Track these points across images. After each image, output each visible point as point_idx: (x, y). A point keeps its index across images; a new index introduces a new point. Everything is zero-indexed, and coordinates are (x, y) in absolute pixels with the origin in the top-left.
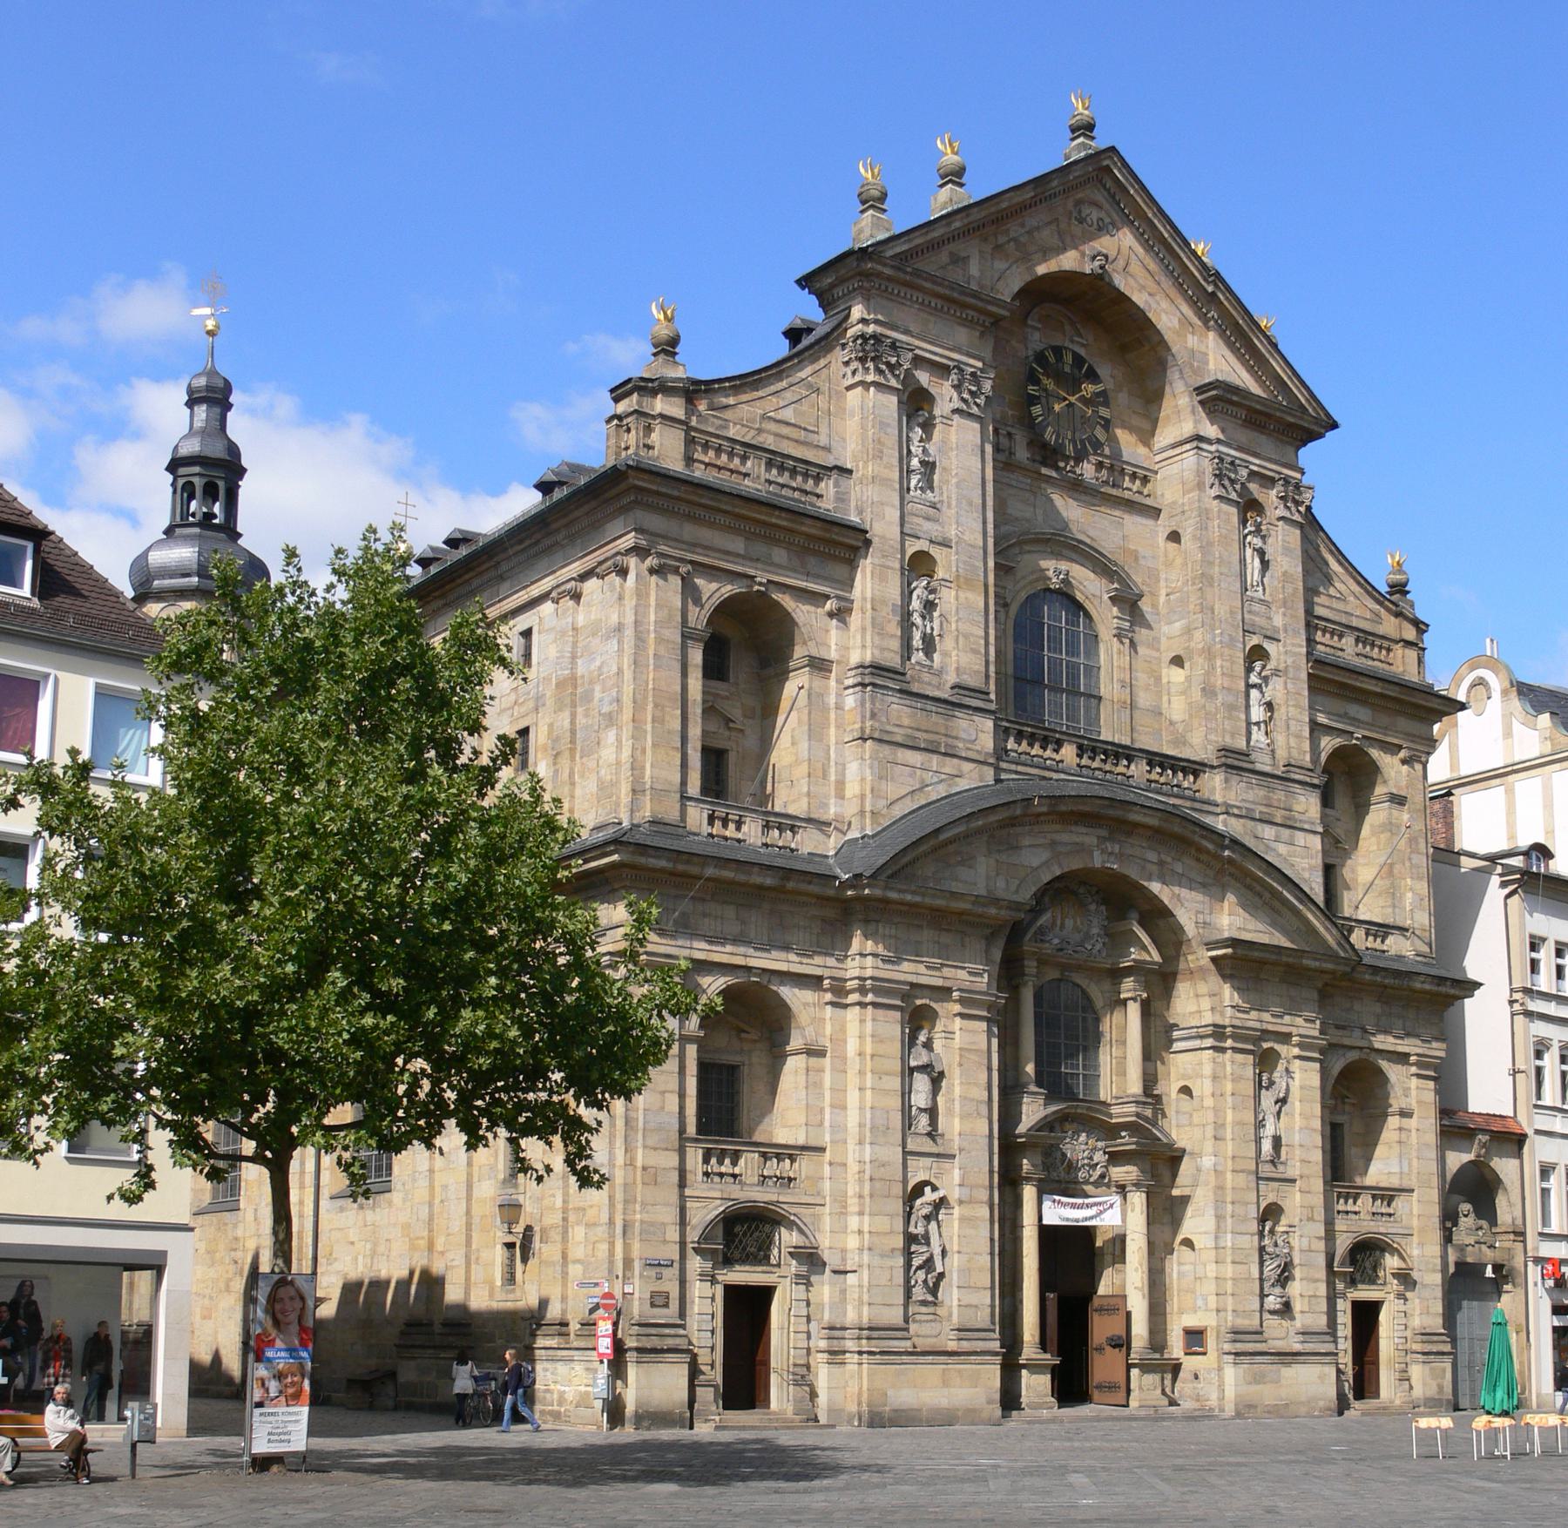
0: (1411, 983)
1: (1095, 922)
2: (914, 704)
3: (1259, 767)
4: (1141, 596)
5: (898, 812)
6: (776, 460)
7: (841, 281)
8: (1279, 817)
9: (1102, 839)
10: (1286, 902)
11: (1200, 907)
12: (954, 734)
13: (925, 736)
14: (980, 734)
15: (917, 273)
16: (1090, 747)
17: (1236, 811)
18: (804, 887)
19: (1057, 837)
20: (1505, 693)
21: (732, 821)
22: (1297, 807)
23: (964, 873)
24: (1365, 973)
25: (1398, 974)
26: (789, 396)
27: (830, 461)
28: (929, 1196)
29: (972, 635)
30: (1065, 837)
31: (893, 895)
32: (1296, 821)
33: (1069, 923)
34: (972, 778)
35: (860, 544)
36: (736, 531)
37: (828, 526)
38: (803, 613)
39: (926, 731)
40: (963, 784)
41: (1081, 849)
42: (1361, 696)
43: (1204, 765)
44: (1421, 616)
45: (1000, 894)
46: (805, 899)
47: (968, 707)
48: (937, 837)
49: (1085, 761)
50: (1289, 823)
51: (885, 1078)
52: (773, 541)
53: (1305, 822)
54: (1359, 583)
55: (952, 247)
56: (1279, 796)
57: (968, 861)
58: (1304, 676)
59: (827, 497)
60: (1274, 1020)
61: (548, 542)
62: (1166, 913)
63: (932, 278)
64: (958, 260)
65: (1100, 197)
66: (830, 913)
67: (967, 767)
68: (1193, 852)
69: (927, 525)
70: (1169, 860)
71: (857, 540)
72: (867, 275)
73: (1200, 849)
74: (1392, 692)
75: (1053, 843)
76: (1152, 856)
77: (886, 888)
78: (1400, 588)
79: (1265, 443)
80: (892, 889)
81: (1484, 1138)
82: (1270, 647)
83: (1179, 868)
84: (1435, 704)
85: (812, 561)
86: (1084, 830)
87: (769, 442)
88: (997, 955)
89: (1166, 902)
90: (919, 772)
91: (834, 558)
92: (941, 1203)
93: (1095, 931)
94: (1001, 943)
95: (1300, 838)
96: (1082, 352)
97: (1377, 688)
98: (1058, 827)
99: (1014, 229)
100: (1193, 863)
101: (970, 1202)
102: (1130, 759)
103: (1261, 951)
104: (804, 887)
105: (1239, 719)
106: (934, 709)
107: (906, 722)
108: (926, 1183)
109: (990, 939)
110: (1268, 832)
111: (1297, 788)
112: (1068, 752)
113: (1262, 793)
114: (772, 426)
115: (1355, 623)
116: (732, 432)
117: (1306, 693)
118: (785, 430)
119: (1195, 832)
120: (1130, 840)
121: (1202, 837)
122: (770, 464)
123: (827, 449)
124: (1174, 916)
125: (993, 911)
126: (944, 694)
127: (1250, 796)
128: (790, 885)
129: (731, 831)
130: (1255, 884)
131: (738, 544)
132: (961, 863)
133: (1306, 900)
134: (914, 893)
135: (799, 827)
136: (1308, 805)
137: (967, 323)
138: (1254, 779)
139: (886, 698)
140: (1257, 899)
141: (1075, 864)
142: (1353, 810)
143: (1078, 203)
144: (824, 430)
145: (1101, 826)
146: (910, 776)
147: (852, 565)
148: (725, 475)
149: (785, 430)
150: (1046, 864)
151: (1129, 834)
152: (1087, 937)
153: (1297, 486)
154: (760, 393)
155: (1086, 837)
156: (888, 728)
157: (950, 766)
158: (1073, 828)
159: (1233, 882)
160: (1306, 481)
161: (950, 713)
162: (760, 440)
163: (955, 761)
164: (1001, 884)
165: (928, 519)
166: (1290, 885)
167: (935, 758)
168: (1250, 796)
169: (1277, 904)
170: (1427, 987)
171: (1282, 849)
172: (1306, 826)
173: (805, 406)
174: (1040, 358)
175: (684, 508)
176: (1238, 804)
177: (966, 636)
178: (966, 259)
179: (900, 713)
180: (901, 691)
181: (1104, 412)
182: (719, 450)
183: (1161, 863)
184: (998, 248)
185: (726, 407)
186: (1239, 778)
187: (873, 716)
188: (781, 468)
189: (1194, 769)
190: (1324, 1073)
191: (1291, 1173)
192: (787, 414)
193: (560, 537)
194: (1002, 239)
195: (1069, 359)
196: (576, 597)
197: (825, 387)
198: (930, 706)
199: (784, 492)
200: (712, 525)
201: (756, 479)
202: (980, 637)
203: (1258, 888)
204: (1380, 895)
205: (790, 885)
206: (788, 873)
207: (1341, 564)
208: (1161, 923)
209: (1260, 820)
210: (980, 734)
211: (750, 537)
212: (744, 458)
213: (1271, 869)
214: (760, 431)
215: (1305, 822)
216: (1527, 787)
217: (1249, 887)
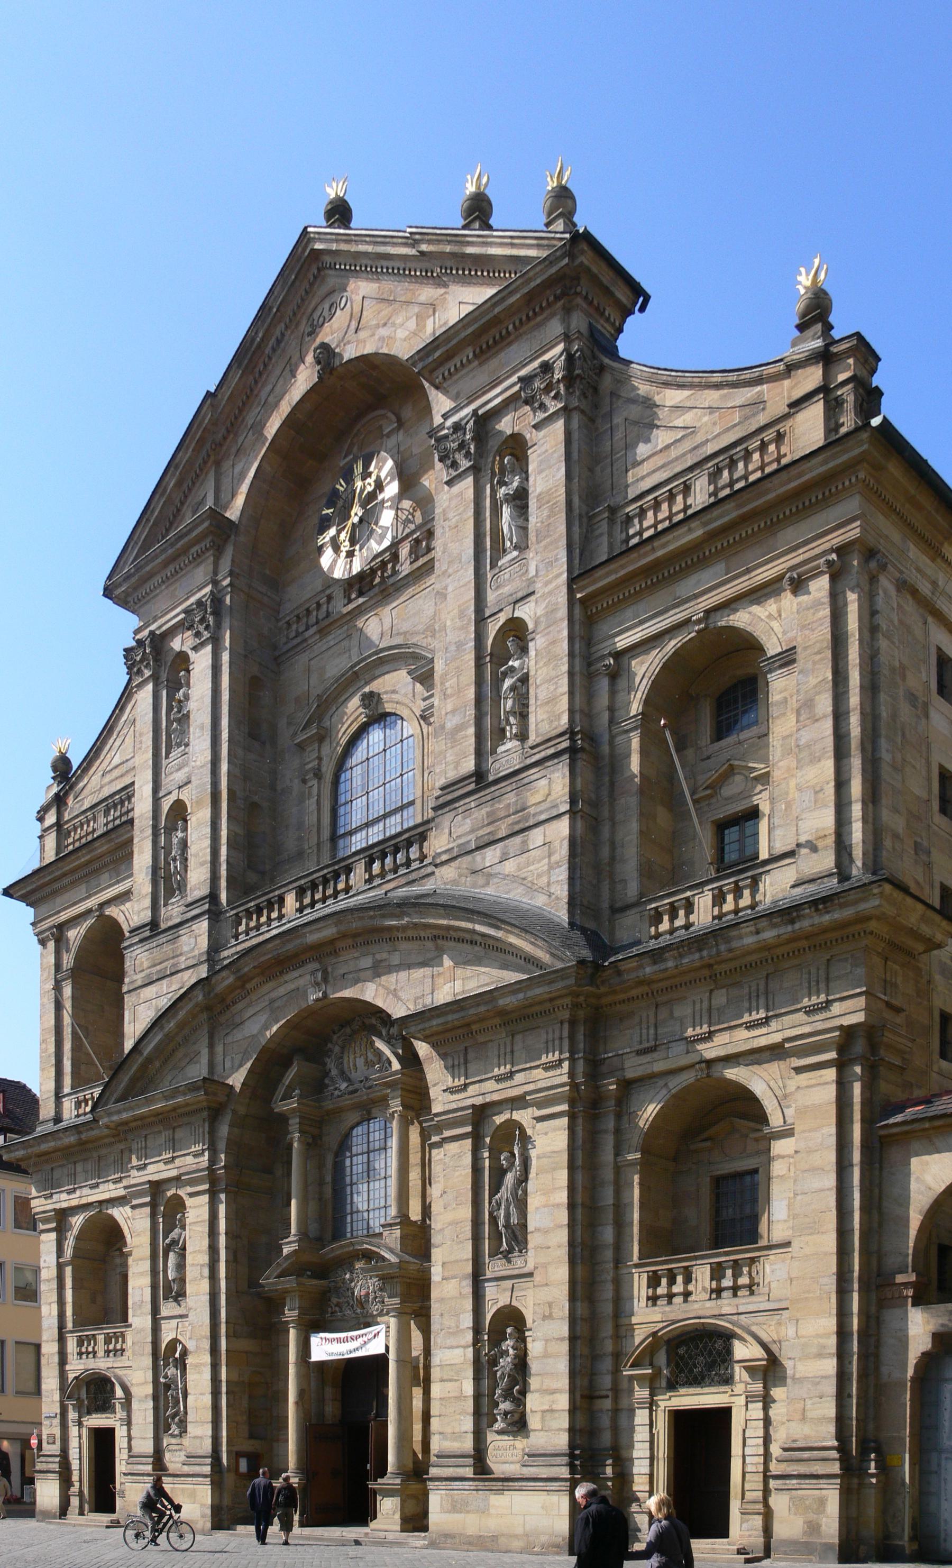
0: (735, 944)
17: (444, 857)
19: (274, 995)
24: (641, 967)
30: (282, 991)
41: (300, 993)
43: (428, 822)
50: (517, 828)
53: (541, 812)
60: (501, 1086)
70: (385, 955)
76: (367, 962)
83: (395, 959)
86: (295, 974)
98: (271, 984)
103: (438, 1016)
110: (491, 855)
113: (484, 811)
120: (341, 959)
145: (303, 963)
158: (287, 977)
170: (769, 935)
171: (509, 867)
186: (452, 814)
209: (478, 848)
215: (541, 812)
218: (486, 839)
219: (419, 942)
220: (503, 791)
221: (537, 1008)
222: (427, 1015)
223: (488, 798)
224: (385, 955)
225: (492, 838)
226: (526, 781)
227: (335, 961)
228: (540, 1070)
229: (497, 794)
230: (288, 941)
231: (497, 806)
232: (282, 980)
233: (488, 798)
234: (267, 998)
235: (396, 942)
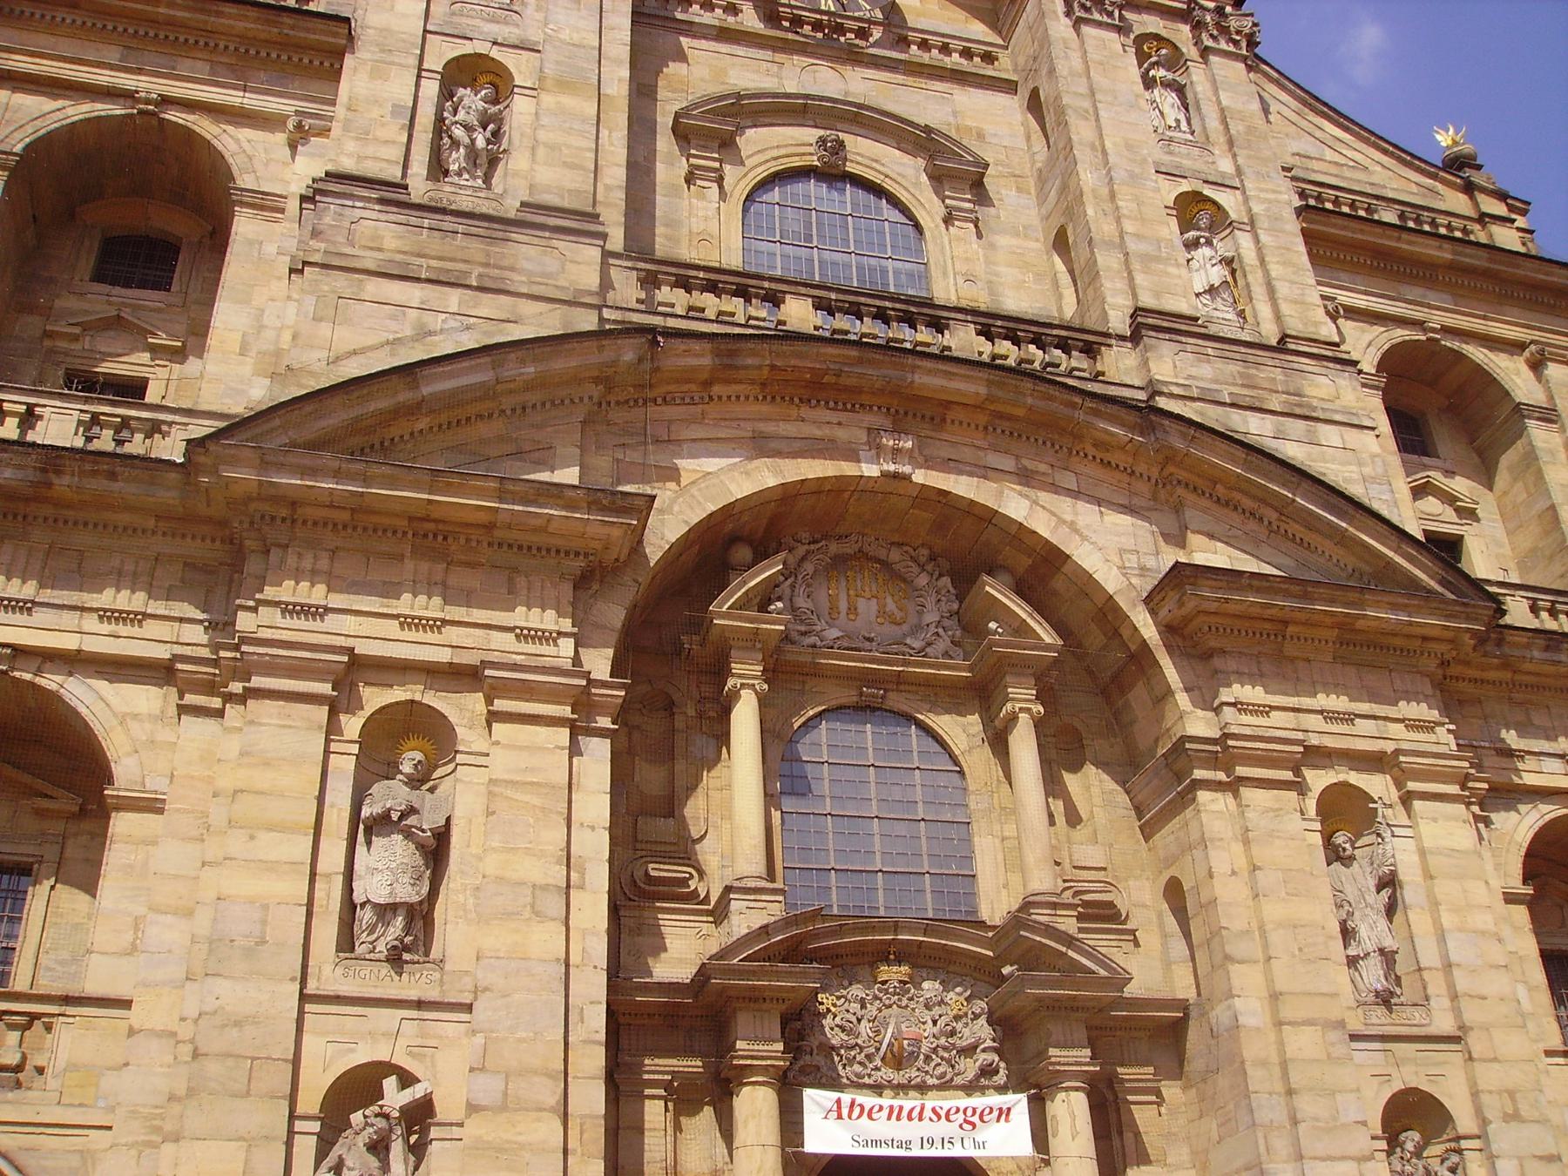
1: (930, 602)
2: (413, 220)
8: (1275, 403)
10: (1311, 522)
11: (1129, 543)
12: (506, 263)
13: (434, 263)
14: (569, 266)
17: (1176, 390)
21: (13, 414)
22: (1309, 391)
24: (1528, 646)
29: (568, 147)
32: (1314, 409)
35: (344, 42)
37: (271, 15)
38: (232, 142)
39: (441, 259)
46: (124, 518)
47: (543, 227)
48: (415, 386)
50: (1298, 411)
51: (264, 837)
53: (1336, 411)
54: (1385, 152)
62: (1052, 558)
66: (195, 549)
68: (1091, 451)
70: (1043, 467)
71: (335, 35)
77: (265, 465)
80: (281, 467)
86: (833, 417)
89: (1044, 532)
90: (413, 314)
97: (1445, 254)
98: (765, 408)
100: (1100, 472)
101: (503, 1108)
103: (1259, 591)
105: (1168, 274)
106: (460, 228)
108: (386, 1068)
113: (1234, 368)
117: (1302, 248)
119: (1073, 406)
120: (945, 436)
121: (1096, 413)
124: (1068, 557)
130: (1237, 496)
133: (1351, 510)
134: (337, 475)
135: (170, 424)
138: (1210, 348)
139: (347, 211)
140: (1252, 525)
142: (1477, 460)
146: (393, 318)
147: (335, 75)
156: (348, 250)
157: (490, 305)
158: (805, 411)
159: (1191, 497)
161: (500, 235)
163: (503, 298)
166: (1306, 485)
167: (453, 299)
169: (1295, 528)
172: (1337, 417)
176: (1181, 381)
177: (552, 147)
180: (381, 201)
186: (1178, 347)
202: (588, 150)
203: (1248, 503)
204: (1551, 558)
207: (1346, 129)
209: (1233, 405)
210: (569, 266)
213: (1253, 458)
215: (1336, 411)
218: (1247, 402)
219: (1126, 478)
220: (1259, 360)
221: (1398, 642)
222: (1245, 581)
223: (1238, 356)
224: (1043, 467)
225: (1257, 404)
226: (1296, 366)
227: (929, 433)
228: (1401, 726)
229: (1251, 358)
230: (871, 362)
231: (1254, 371)
232: (794, 412)
233: (1238, 356)
234: (749, 426)
235: (1075, 459)
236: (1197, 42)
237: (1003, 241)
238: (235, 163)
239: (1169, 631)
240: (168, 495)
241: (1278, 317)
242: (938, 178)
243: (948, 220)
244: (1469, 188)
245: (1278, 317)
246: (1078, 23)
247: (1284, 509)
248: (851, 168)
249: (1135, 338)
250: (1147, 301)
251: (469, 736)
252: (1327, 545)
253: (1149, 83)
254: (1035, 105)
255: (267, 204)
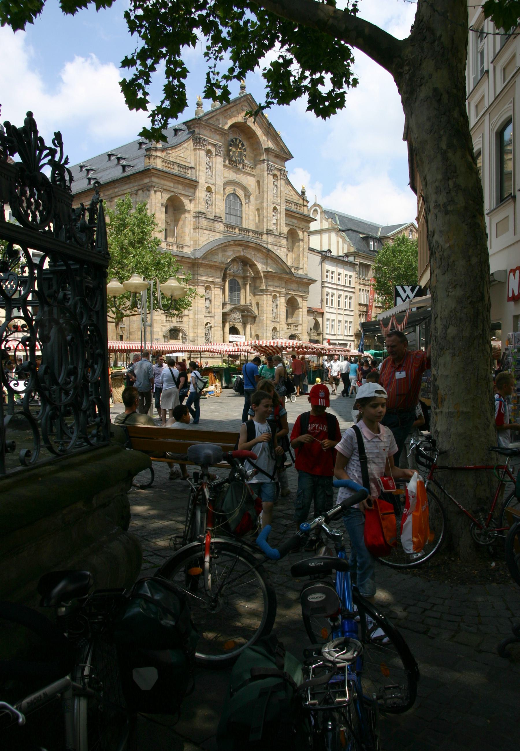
3: (275, 233)
4: (251, 194)
5: (204, 244)
6: (180, 166)
7: (193, 124)
9: (243, 249)
10: (279, 263)
15: (210, 123)
16: (241, 229)
18: (186, 260)
20: (321, 213)
23: (216, 257)
25: (301, 278)
26: (182, 151)
27: (190, 166)
28: (209, 325)
30: (236, 249)
31: (203, 262)
33: (235, 267)
34: (218, 236)
36: (172, 182)
40: (217, 238)
41: (239, 251)
42: (295, 218)
44: (308, 200)
45: (223, 261)
49: (241, 232)
52: (179, 184)
55: (217, 117)
56: (278, 240)
57: (217, 254)
58: (284, 213)
59: (190, 174)
61: (129, 181)
63: (213, 125)
64: (218, 120)
65: (246, 104)
66: (190, 265)
67: (217, 234)
69: (210, 180)
72: (200, 124)
73: (263, 252)
74: (302, 217)
75: (234, 250)
76: (253, 253)
78: (303, 193)
79: (278, 161)
81: (316, 313)
82: (278, 207)
83: (258, 255)
84: (310, 219)
85: (187, 188)
87: (178, 161)
88: (222, 274)
91: (191, 187)
92: (211, 327)
93: (240, 268)
94: (223, 271)
95: (282, 249)
96: (240, 139)
99: (229, 112)
102: (249, 232)
104: (186, 260)
107: (206, 224)
108: (208, 323)
109: (221, 271)
110: (276, 248)
111: (282, 238)
112: (237, 230)
113: (275, 239)
114: (178, 158)
115: (295, 201)
116: (171, 159)
118: (181, 159)
122: (178, 166)
123: (190, 163)
125: (222, 265)
126: (213, 218)
127: (273, 240)
128: (183, 260)
129: (171, 248)
131: (172, 185)
132: (216, 255)
136: (284, 242)
137: (219, 134)
138: (274, 236)
141: (238, 255)
143: (242, 106)
144: (189, 159)
148: (169, 169)
149: (181, 159)
150: (232, 255)
151: (249, 248)
152: (238, 270)
153: (284, 171)
154: (176, 150)
155: (240, 249)
157: (214, 234)
160: (286, 170)
162: (176, 161)
164: (223, 259)
165: (210, 179)
168: (273, 240)
171: (279, 251)
173: (185, 153)
174: (232, 141)
175: (162, 177)
178: (219, 120)
179: (204, 222)
181: (245, 153)
182: (168, 163)
183: (255, 254)
184: (225, 116)
185: (170, 154)
187: (199, 223)
188: (181, 167)
189: (261, 234)
190: (285, 299)
191: (278, 320)
192: (182, 155)
193: (132, 181)
194: (226, 114)
195: (238, 141)
196: (136, 194)
197: (189, 149)
198: (210, 221)
199: (182, 173)
200: (167, 180)
201: (176, 170)
205: (183, 260)
206: (183, 257)
208: (254, 267)
211: (174, 183)
212: (173, 165)
214: (176, 159)
216: (325, 236)
217: (272, 260)
236: (280, 176)
237: (250, 207)
238: (185, 204)
239: (264, 275)
240: (191, 261)
241: (280, 229)
242: (245, 195)
243: (245, 204)
244: (303, 199)
245: (280, 229)
246: (268, 174)
247: (277, 261)
248: (237, 193)
249: (267, 234)
250: (269, 228)
251: (213, 289)
252: (279, 265)
253: (274, 184)
254: (258, 182)
255: (189, 212)
